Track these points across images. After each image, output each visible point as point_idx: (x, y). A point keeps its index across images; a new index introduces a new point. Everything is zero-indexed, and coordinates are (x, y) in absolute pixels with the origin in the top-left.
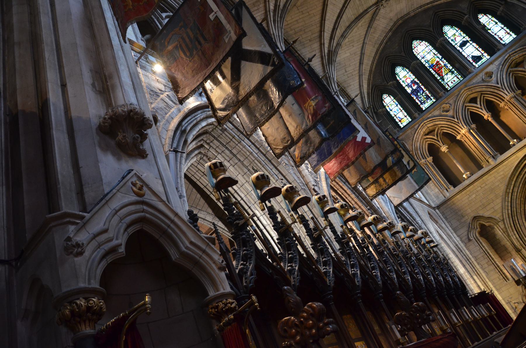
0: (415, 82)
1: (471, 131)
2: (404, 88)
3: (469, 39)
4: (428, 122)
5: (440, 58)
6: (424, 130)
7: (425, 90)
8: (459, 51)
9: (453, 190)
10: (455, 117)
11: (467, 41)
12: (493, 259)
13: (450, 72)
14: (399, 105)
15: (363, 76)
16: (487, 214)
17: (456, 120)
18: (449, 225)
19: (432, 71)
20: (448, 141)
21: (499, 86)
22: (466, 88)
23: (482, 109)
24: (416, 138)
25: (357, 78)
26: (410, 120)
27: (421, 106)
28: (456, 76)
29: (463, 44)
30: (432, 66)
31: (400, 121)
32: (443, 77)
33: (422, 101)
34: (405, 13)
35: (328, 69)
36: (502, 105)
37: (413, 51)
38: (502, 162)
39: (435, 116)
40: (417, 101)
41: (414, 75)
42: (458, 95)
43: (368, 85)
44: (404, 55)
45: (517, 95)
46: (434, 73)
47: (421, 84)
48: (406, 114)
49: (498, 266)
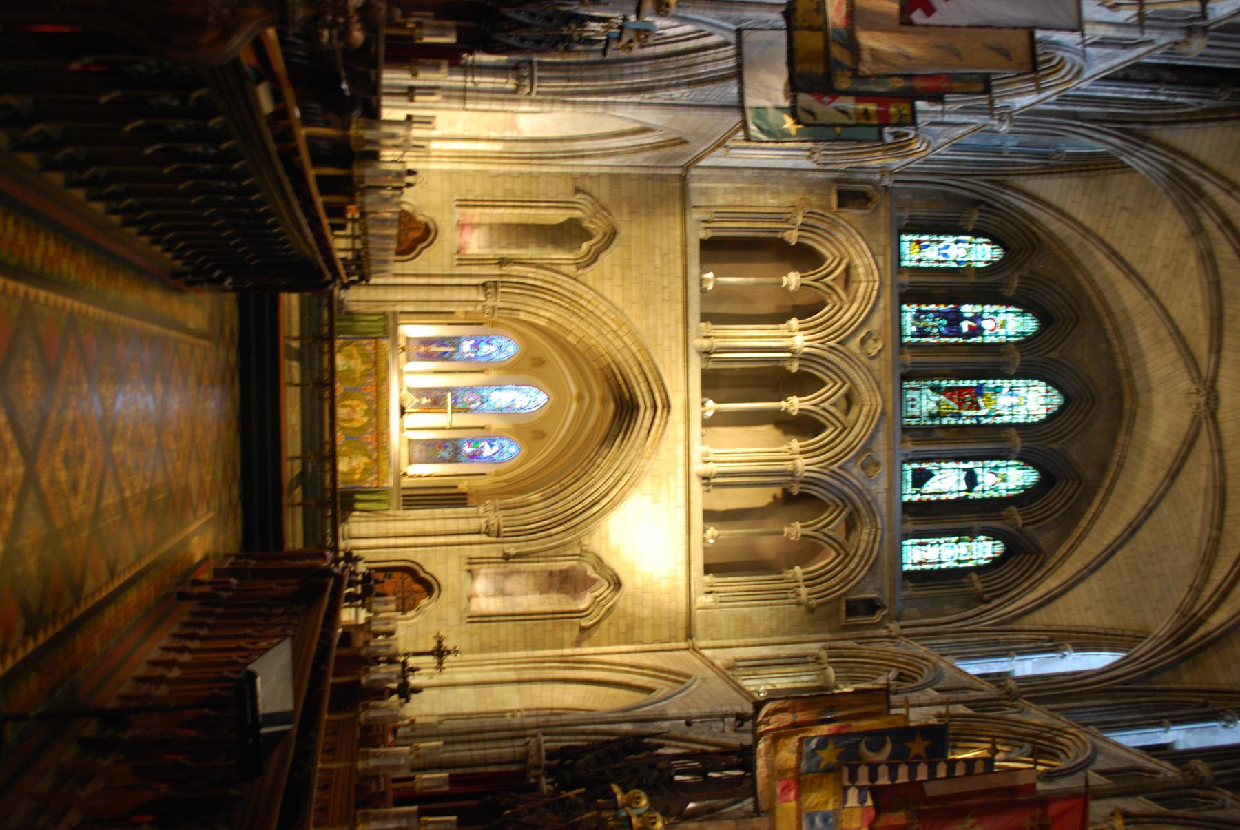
0: (976, 336)
1: (788, 355)
2: (983, 303)
3: (971, 495)
4: (872, 290)
5: (981, 419)
6: (861, 270)
7: (943, 340)
8: (965, 460)
9: (699, 233)
10: (840, 347)
11: (970, 490)
12: (515, 207)
13: (938, 412)
14: (954, 265)
15: (1079, 238)
16: (606, 259)
17: (832, 343)
18: (634, 175)
19: (967, 383)
20: (802, 300)
21: (834, 467)
22: (879, 410)
23: (815, 405)
24: (857, 242)
25: (1087, 222)
26: (904, 264)
27: (914, 308)
29: (971, 479)
30: (979, 391)
31: (918, 242)
32: (941, 394)
33: (923, 316)
34: (1137, 429)
35: (1163, 159)
36: (795, 444)
37: (1043, 383)
38: (687, 360)
39: (872, 311)
40: (933, 307)
41: (992, 344)
42: (879, 388)
43: (1050, 235)
44: (1050, 355)
45: (794, 481)
46: (961, 383)
47: (961, 340)
48: (923, 264)
49: (494, 206)
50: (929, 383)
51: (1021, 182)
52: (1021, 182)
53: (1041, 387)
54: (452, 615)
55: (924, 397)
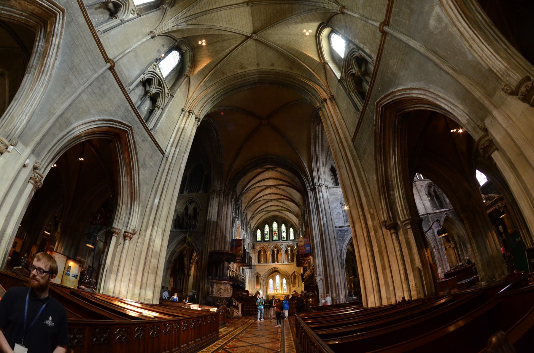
29: (284, 232)
30: (274, 231)
51: (252, 229)
52: (252, 229)
54: (298, 289)
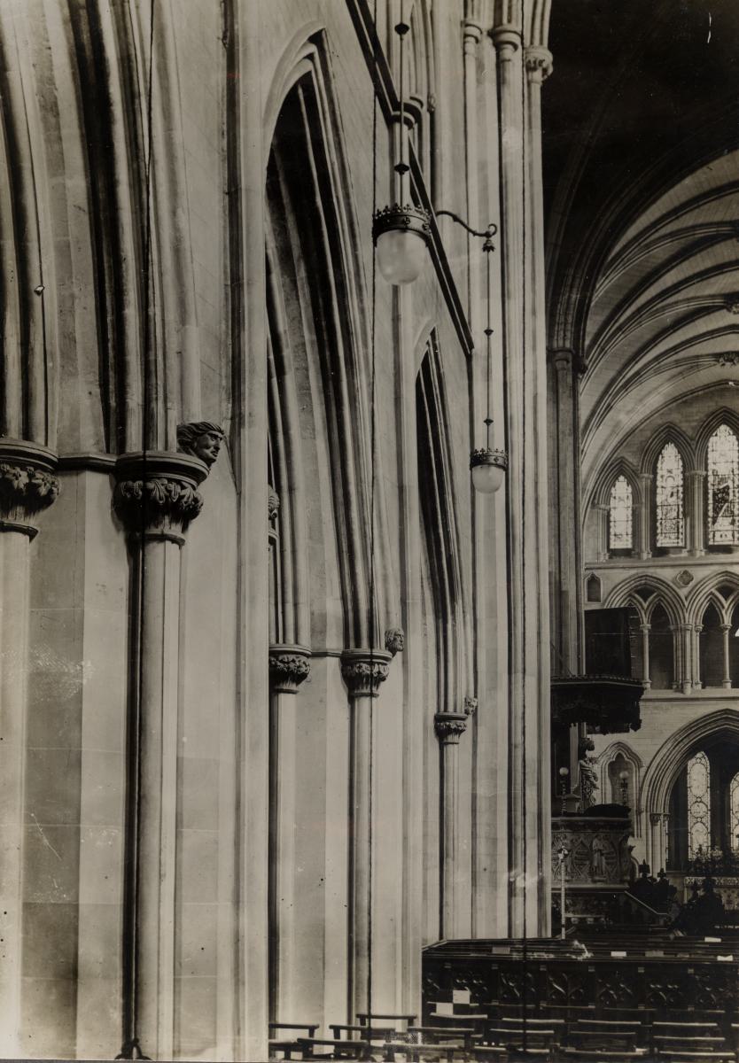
27: (659, 537)
28: (733, 531)
44: (694, 447)
50: (710, 525)
53: (713, 440)
55: (719, 528)
